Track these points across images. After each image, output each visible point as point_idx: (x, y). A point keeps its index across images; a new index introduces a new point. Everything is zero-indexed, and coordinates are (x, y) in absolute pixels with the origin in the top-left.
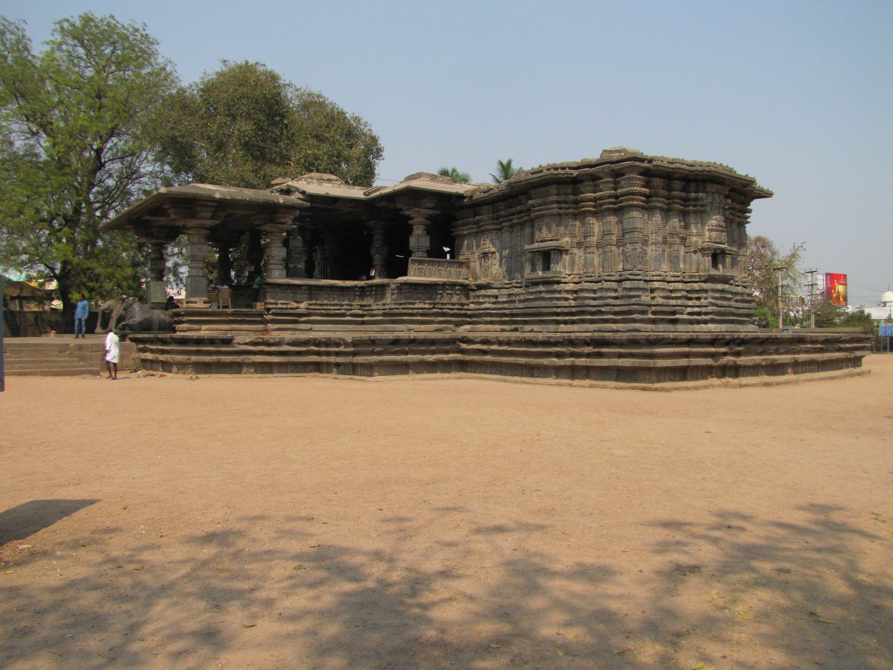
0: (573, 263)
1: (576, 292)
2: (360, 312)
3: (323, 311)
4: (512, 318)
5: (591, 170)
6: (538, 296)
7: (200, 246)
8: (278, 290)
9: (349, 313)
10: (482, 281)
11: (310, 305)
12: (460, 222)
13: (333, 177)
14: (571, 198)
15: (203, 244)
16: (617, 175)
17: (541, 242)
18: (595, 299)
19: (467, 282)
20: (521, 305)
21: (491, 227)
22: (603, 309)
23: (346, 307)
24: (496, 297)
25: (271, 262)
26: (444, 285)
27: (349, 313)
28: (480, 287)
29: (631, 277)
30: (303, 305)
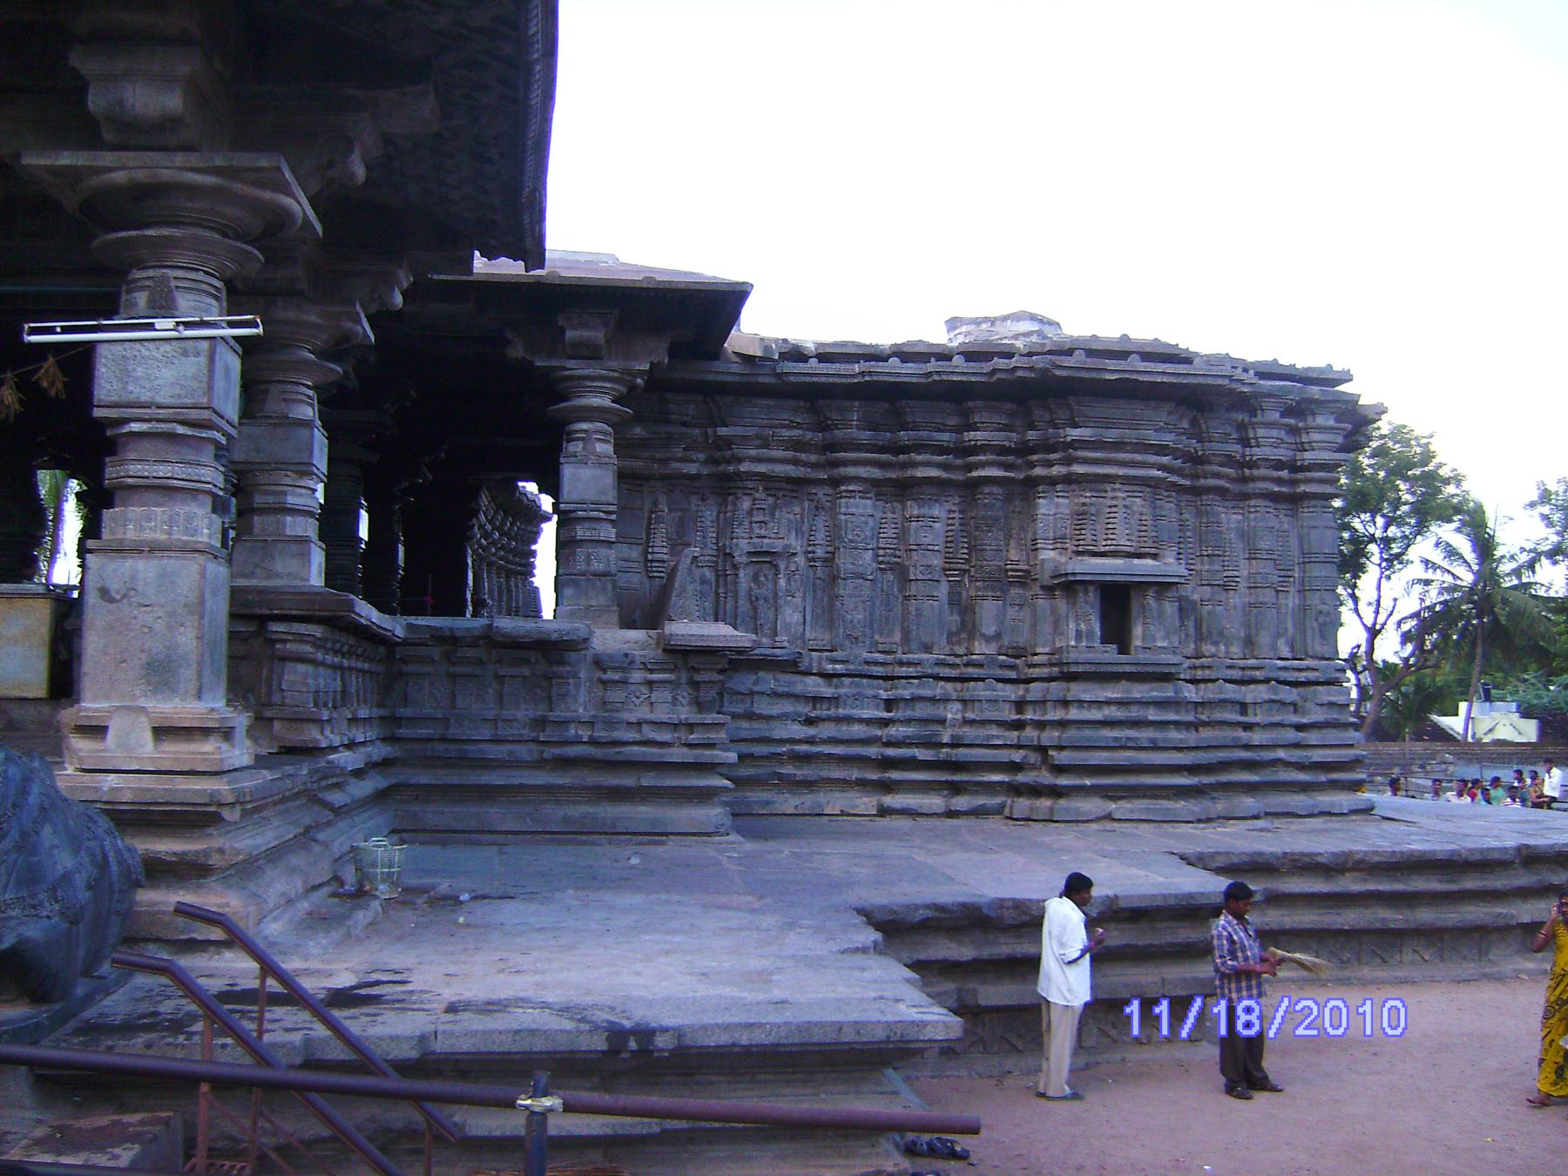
18: (1248, 727)
22: (1281, 754)
24: (815, 700)
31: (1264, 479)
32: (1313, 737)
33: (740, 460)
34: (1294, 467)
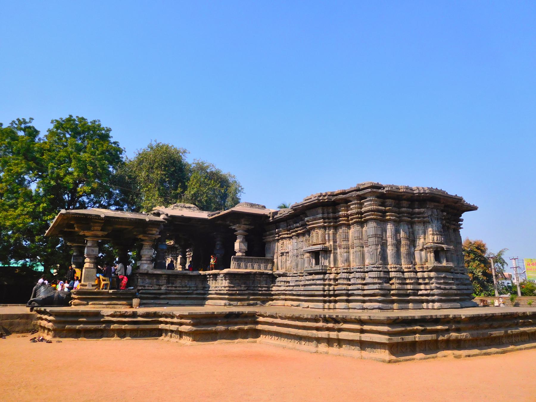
0: (335, 260)
1: (337, 280)
2: (202, 292)
3: (177, 292)
4: (298, 297)
5: (344, 196)
6: (314, 282)
7: (93, 249)
8: (146, 277)
9: (195, 292)
10: (281, 272)
11: (168, 287)
12: (268, 233)
13: (192, 206)
14: (331, 215)
15: (96, 247)
16: (361, 198)
17: (314, 245)
19: (270, 272)
20: (302, 288)
21: (286, 236)
23: (193, 288)
24: (289, 282)
25: (143, 259)
26: (255, 274)
27: (195, 292)
28: (280, 275)
29: (374, 269)
30: (163, 288)
31: (354, 218)
32: (366, 287)
33: (281, 235)
34: (361, 213)
